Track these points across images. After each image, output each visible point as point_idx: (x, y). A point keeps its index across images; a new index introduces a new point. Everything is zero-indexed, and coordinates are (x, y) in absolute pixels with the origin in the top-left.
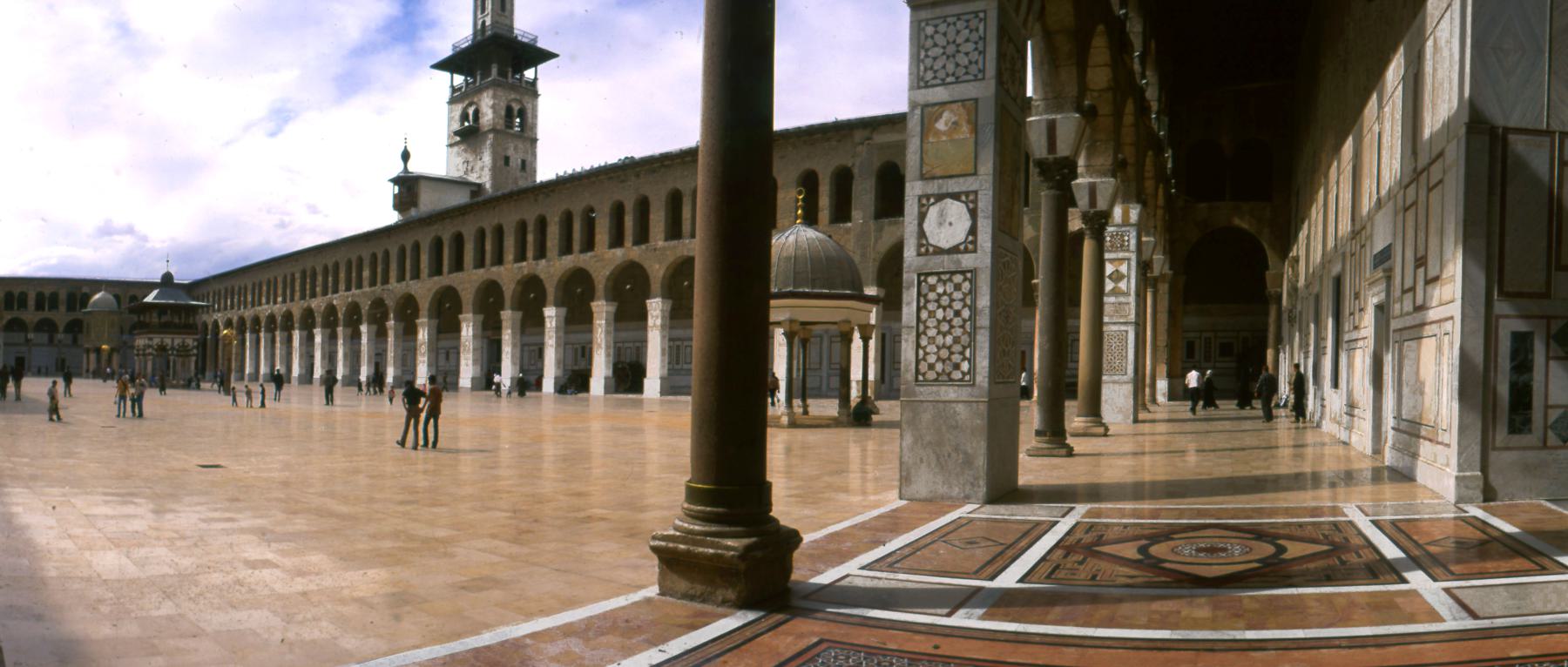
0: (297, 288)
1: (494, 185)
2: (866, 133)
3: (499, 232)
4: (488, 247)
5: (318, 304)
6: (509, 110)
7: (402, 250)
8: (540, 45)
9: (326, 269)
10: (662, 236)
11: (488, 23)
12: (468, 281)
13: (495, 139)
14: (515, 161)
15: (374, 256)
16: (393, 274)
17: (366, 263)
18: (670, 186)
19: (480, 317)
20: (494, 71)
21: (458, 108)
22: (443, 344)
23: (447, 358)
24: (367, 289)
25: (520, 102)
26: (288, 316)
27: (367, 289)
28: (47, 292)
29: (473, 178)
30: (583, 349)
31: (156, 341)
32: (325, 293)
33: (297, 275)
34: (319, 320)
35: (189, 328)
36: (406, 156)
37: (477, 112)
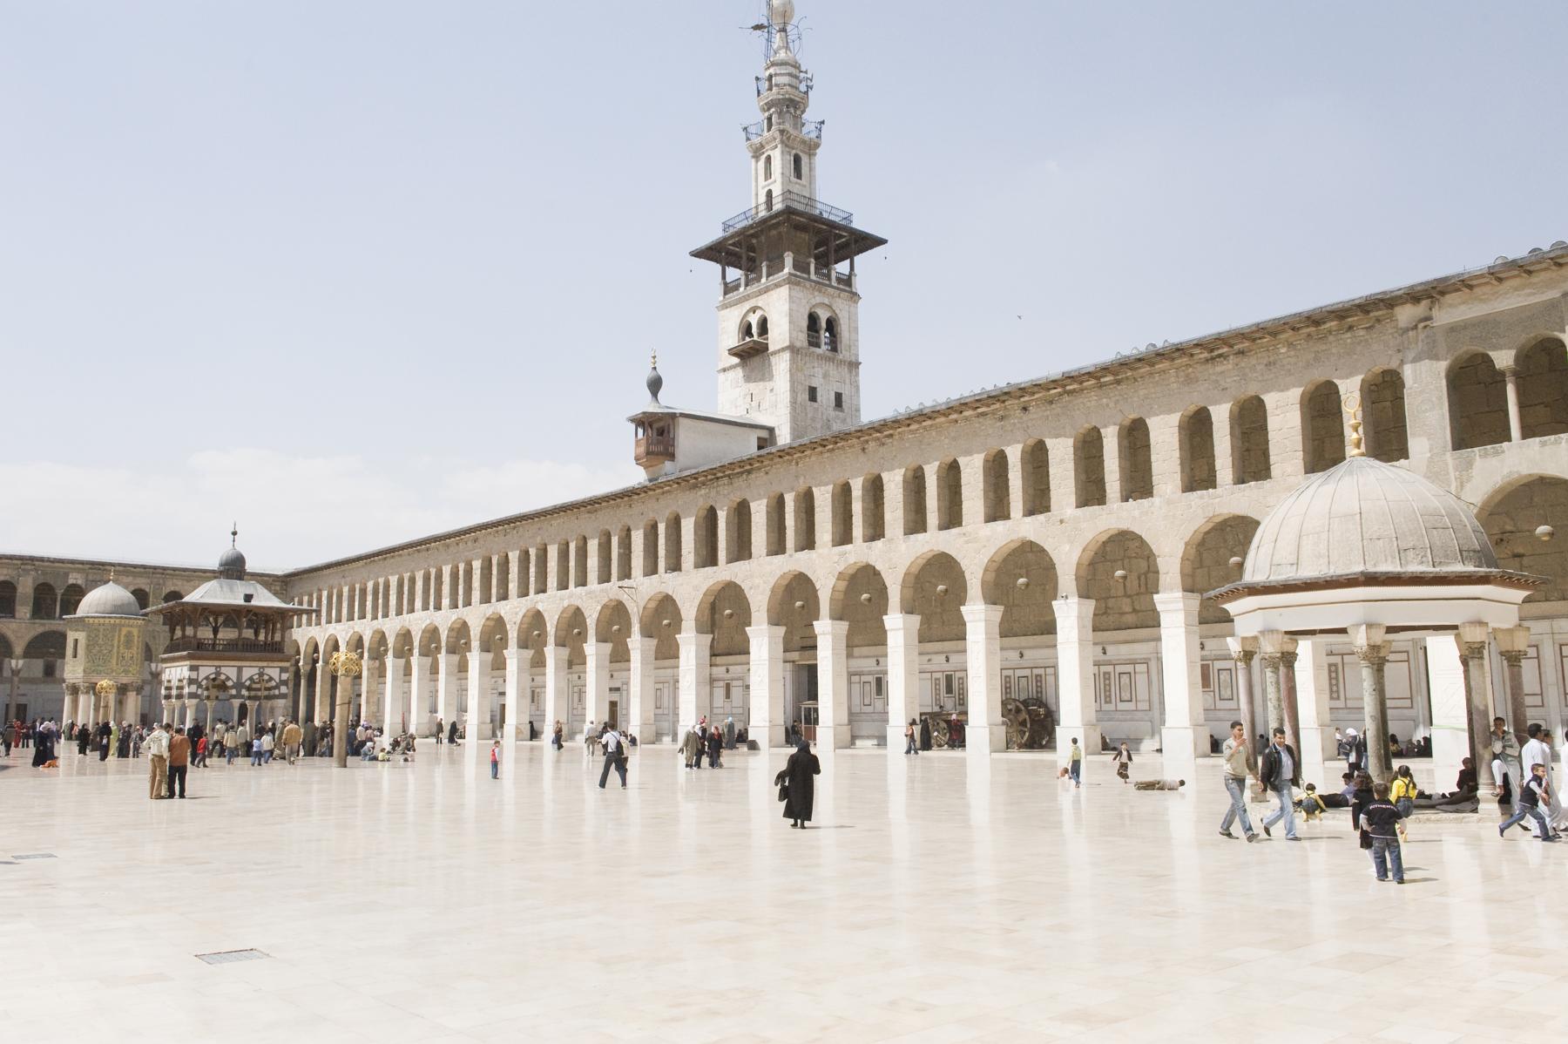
0: (476, 583)
1: (796, 431)
5: (513, 610)
6: (813, 319)
8: (858, 225)
10: (1073, 499)
11: (777, 192)
12: (760, 576)
13: (793, 361)
14: (826, 397)
19: (781, 631)
20: (789, 259)
22: (719, 671)
23: (728, 696)
25: (830, 307)
26: (462, 630)
30: (949, 679)
31: (207, 670)
32: (524, 593)
34: (513, 635)
35: (274, 650)
36: (655, 385)
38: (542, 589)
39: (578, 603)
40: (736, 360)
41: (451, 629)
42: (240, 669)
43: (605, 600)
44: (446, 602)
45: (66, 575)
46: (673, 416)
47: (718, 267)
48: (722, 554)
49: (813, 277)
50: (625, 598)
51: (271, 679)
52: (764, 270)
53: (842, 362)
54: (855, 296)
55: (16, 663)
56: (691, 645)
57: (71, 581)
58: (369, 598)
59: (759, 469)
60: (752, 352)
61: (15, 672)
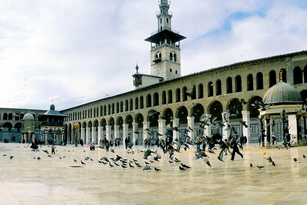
0: (99, 112)
2: (289, 58)
3: (170, 92)
4: (167, 97)
6: (171, 54)
7: (137, 99)
9: (109, 106)
10: (226, 92)
15: (127, 101)
16: (134, 107)
17: (124, 103)
18: (227, 76)
21: (154, 53)
24: (124, 112)
25: (174, 52)
26: (96, 122)
27: (124, 112)
28: (8, 113)
29: (159, 76)
31: (49, 128)
32: (109, 114)
33: (99, 108)
34: (107, 123)
35: (61, 124)
37: (160, 55)
38: (113, 113)
39: (121, 116)
40: (154, 63)
41: (94, 122)
42: (55, 128)
43: (127, 115)
44: (93, 116)
45: (21, 112)
46: (141, 75)
47: (150, 43)
48: (152, 105)
49: (171, 45)
50: (131, 114)
51: (61, 130)
52: (161, 43)
53: (177, 64)
54: (179, 50)
55: (13, 129)
56: (146, 125)
57: (22, 113)
58: (77, 116)
59: (160, 86)
60: (158, 61)
61: (13, 130)
